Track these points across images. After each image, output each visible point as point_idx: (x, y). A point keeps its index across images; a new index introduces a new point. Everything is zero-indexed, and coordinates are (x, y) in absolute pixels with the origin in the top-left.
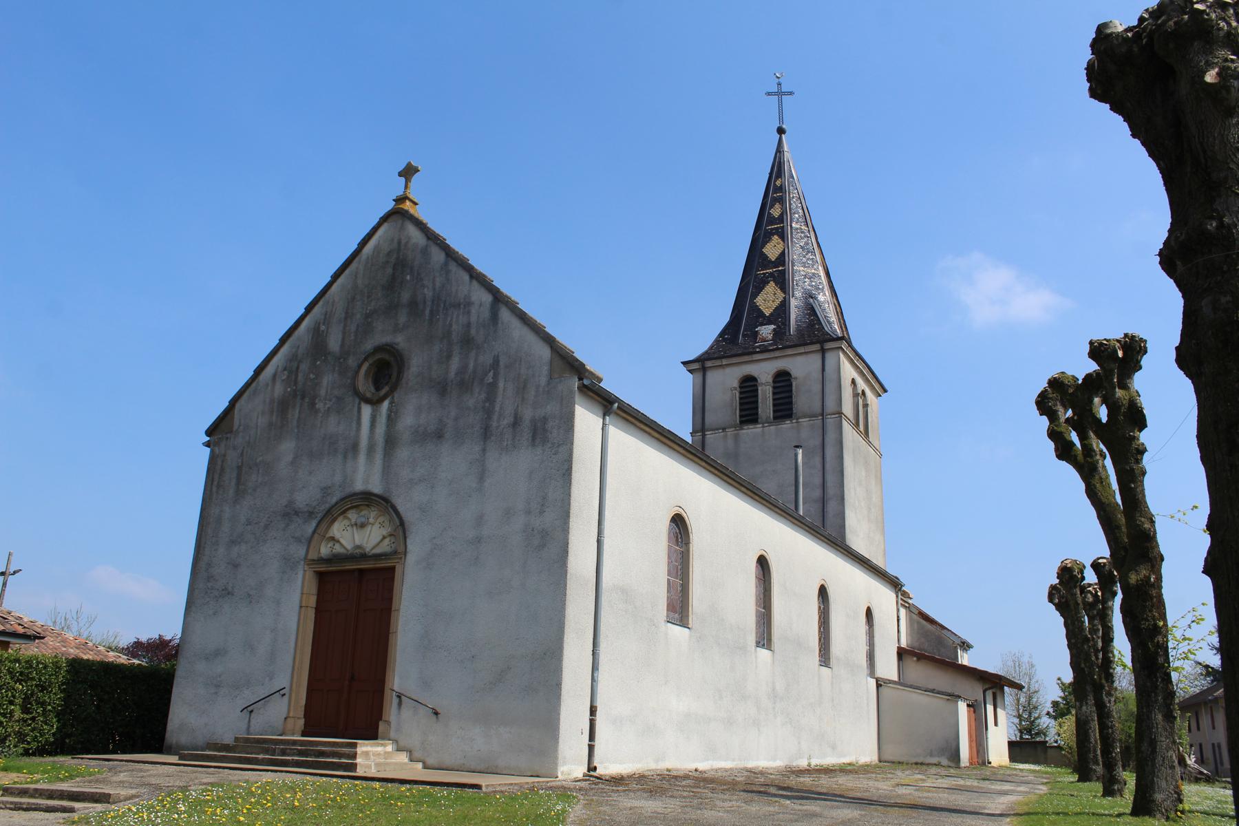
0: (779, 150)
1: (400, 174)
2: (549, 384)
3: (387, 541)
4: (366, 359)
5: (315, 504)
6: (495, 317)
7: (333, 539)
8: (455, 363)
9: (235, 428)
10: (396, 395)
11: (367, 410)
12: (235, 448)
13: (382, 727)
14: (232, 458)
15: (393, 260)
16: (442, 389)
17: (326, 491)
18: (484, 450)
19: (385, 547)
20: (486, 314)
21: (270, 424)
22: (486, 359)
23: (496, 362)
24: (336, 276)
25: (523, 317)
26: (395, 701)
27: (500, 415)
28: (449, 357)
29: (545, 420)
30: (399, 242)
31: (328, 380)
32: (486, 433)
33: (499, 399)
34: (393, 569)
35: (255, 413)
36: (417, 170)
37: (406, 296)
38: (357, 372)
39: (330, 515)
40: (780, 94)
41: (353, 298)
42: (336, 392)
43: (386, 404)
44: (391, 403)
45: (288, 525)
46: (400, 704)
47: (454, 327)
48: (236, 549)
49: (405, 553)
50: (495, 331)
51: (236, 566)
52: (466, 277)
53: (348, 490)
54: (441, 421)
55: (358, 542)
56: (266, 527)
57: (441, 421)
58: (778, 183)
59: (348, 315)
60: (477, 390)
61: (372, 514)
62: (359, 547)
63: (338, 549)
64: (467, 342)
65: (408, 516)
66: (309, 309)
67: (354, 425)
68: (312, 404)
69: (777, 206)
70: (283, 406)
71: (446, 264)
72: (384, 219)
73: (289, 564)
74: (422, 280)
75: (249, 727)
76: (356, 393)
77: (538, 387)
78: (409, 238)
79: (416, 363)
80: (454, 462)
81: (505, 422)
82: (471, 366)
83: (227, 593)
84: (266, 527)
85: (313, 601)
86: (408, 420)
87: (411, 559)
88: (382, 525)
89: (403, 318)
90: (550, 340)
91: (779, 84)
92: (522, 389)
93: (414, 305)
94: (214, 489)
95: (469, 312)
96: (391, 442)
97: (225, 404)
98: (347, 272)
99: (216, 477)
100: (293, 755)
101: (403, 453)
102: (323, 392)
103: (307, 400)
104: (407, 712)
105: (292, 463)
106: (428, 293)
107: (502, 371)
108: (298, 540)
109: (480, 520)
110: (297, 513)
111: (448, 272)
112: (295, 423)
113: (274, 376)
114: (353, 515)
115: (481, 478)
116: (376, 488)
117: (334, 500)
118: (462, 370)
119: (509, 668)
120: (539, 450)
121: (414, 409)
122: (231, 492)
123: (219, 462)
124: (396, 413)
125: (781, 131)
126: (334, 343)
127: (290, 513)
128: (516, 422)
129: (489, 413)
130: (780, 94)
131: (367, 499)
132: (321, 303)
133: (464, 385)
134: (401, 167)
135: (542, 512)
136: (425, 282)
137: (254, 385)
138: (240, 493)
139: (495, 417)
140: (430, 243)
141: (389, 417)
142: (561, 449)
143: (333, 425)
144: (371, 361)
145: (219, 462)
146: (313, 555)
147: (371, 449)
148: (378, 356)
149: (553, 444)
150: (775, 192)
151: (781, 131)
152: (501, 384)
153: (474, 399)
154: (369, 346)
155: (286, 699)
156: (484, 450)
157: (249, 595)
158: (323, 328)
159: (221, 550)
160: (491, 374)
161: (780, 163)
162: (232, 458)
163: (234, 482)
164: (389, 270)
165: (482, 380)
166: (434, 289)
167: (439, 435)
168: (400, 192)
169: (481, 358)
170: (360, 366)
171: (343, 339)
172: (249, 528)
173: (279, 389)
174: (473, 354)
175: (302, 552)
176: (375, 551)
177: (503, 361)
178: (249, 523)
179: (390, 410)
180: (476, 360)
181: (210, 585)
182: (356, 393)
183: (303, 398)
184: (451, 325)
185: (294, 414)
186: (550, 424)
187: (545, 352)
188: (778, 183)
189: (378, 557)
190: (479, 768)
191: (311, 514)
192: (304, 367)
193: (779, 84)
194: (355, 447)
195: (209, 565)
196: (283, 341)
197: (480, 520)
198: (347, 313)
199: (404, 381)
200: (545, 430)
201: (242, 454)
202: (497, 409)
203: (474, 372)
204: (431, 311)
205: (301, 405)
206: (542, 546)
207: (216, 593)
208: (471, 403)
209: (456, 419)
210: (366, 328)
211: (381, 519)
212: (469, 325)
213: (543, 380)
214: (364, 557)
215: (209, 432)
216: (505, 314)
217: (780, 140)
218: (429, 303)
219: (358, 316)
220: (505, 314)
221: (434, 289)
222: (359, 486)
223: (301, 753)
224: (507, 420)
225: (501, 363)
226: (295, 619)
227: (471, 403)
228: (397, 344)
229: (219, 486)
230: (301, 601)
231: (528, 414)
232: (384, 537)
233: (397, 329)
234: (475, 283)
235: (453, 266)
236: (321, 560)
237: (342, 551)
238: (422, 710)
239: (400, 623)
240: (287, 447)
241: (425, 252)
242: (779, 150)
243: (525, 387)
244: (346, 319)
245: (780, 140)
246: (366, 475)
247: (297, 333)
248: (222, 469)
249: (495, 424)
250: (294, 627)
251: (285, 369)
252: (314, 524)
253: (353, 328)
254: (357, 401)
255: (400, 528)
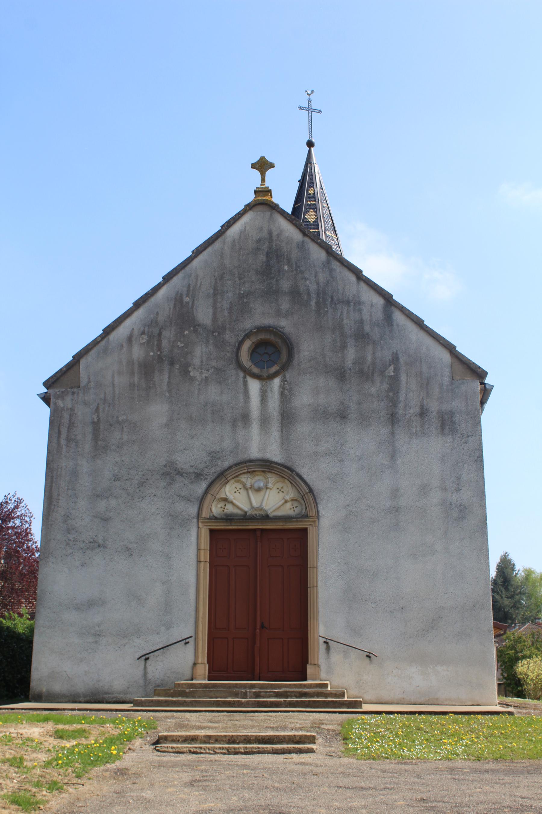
0: (309, 161)
1: (254, 166)
2: (452, 384)
3: (289, 505)
4: (247, 336)
5: (202, 466)
6: (388, 319)
7: (226, 500)
8: (351, 355)
9: (84, 381)
10: (288, 375)
11: (254, 386)
12: (85, 404)
13: (310, 670)
14: (83, 414)
15: (265, 247)
16: (341, 375)
17: (214, 456)
18: (392, 433)
19: (288, 510)
20: (379, 315)
21: (132, 386)
22: (385, 354)
23: (395, 359)
24: (198, 252)
25: (419, 323)
26: (322, 647)
27: (406, 406)
28: (344, 347)
29: (452, 413)
30: (270, 233)
31: (200, 352)
32: (393, 419)
33: (403, 391)
34: (305, 531)
35: (109, 371)
36: (272, 166)
37: (285, 284)
38: (239, 348)
39: (222, 477)
40: (310, 110)
41: (222, 277)
42: (214, 363)
43: (277, 381)
44: (284, 381)
45: (170, 484)
46: (328, 648)
47: (345, 321)
48: (102, 505)
49: (318, 517)
50: (391, 331)
51: (106, 520)
52: (353, 278)
53: (242, 457)
54: (342, 403)
55: (255, 504)
56: (141, 484)
57: (342, 403)
58: (311, 191)
59: (217, 293)
60: (378, 380)
61: (272, 480)
62: (259, 509)
63: (230, 509)
64: (362, 337)
65: (316, 485)
66: (167, 278)
67: (241, 396)
68: (185, 372)
69: (311, 212)
70: (147, 369)
71: (328, 262)
72: (249, 207)
73: (176, 521)
74: (302, 272)
75: (145, 674)
76: (240, 366)
77: (441, 385)
78: (281, 231)
79: (307, 348)
80: (362, 441)
81: (412, 411)
82: (369, 358)
83: (97, 545)
84: (141, 484)
85: (205, 556)
86: (304, 399)
87: (325, 522)
88: (280, 490)
89: (285, 304)
90: (450, 348)
91: (310, 101)
92: (426, 384)
93: (296, 295)
94: (63, 442)
95: (360, 311)
96: (287, 418)
97: (69, 359)
98: (210, 250)
99: (64, 431)
100: (269, 697)
101: (302, 428)
102: (197, 362)
103: (177, 366)
104: (336, 657)
105: (167, 425)
106: (313, 288)
107: (403, 368)
108: (187, 499)
109: (395, 493)
110: (180, 473)
111: (331, 271)
112: (165, 387)
113: (130, 339)
114: (248, 480)
115: (393, 456)
116: (275, 454)
117: (226, 464)
118: (360, 361)
119: (440, 617)
120: (449, 439)
121: (310, 392)
122: (88, 446)
123: (66, 416)
124: (290, 390)
125: (310, 144)
126: (204, 314)
127: (171, 473)
128: (423, 413)
129: (394, 403)
130: (310, 110)
131: (266, 466)
132: (181, 275)
133: (365, 374)
134: (255, 160)
135: (458, 490)
136: (307, 276)
137: (103, 343)
138: (100, 447)
139: (401, 405)
140: (307, 239)
141: (282, 394)
142: (470, 439)
143: (213, 393)
144: (254, 339)
145: (66, 416)
146: (205, 514)
147: (265, 421)
148: (262, 336)
149: (463, 435)
150: (309, 199)
151: (310, 144)
152: (403, 378)
153: (377, 387)
154: (248, 324)
155: (190, 647)
156: (392, 433)
157: (128, 549)
158: (186, 299)
159: (83, 503)
160: (392, 368)
161: (311, 173)
162: (83, 414)
163: (89, 437)
164: (262, 258)
165: (382, 373)
166: (318, 284)
167: (342, 415)
168: (258, 184)
169: (379, 354)
170: (241, 343)
171: (215, 314)
172: (118, 483)
173: (138, 352)
174: (370, 348)
175: (193, 510)
176: (279, 513)
177: (402, 359)
178: (116, 478)
179: (282, 388)
180: (374, 354)
181: (71, 537)
182: (240, 366)
183: (172, 363)
184: (343, 320)
185: (162, 378)
186: (457, 418)
187: (446, 357)
188: (311, 191)
189: (287, 519)
190: (419, 701)
191: (198, 476)
192: (169, 334)
193: (310, 101)
194: (245, 418)
195: (67, 518)
196: (138, 304)
197: (395, 493)
198: (215, 289)
199: (295, 362)
200: (453, 423)
201: (97, 410)
202: (402, 398)
203: (374, 364)
204: (318, 303)
205: (170, 372)
206: (462, 517)
207: (82, 545)
208: (373, 390)
209: (359, 403)
210: (242, 305)
211: (280, 485)
212: (361, 321)
213: (446, 380)
214: (266, 518)
215: (48, 384)
216: (398, 316)
217: (310, 153)
218: (314, 295)
219: (230, 295)
220: (398, 316)
221: (318, 284)
222: (255, 453)
223: (278, 695)
224: (414, 410)
225: (401, 360)
226: (193, 572)
227: (373, 390)
228: (283, 328)
229: (69, 440)
230: (198, 555)
231: (434, 407)
232: (286, 502)
233: (279, 313)
234: (362, 284)
235: (335, 265)
236: (214, 519)
237: (236, 511)
238: (353, 654)
239: (320, 578)
240: (158, 411)
241: (301, 246)
242: (309, 161)
243: (428, 383)
244: (215, 295)
245: (310, 153)
246: (261, 443)
247: (153, 300)
248: (71, 425)
249: (401, 412)
250: (193, 580)
251: (143, 333)
252: (204, 485)
253: (226, 305)
254: (241, 374)
255: (307, 495)
